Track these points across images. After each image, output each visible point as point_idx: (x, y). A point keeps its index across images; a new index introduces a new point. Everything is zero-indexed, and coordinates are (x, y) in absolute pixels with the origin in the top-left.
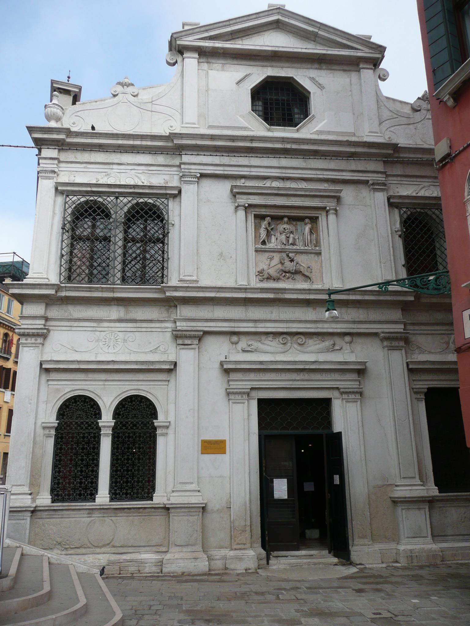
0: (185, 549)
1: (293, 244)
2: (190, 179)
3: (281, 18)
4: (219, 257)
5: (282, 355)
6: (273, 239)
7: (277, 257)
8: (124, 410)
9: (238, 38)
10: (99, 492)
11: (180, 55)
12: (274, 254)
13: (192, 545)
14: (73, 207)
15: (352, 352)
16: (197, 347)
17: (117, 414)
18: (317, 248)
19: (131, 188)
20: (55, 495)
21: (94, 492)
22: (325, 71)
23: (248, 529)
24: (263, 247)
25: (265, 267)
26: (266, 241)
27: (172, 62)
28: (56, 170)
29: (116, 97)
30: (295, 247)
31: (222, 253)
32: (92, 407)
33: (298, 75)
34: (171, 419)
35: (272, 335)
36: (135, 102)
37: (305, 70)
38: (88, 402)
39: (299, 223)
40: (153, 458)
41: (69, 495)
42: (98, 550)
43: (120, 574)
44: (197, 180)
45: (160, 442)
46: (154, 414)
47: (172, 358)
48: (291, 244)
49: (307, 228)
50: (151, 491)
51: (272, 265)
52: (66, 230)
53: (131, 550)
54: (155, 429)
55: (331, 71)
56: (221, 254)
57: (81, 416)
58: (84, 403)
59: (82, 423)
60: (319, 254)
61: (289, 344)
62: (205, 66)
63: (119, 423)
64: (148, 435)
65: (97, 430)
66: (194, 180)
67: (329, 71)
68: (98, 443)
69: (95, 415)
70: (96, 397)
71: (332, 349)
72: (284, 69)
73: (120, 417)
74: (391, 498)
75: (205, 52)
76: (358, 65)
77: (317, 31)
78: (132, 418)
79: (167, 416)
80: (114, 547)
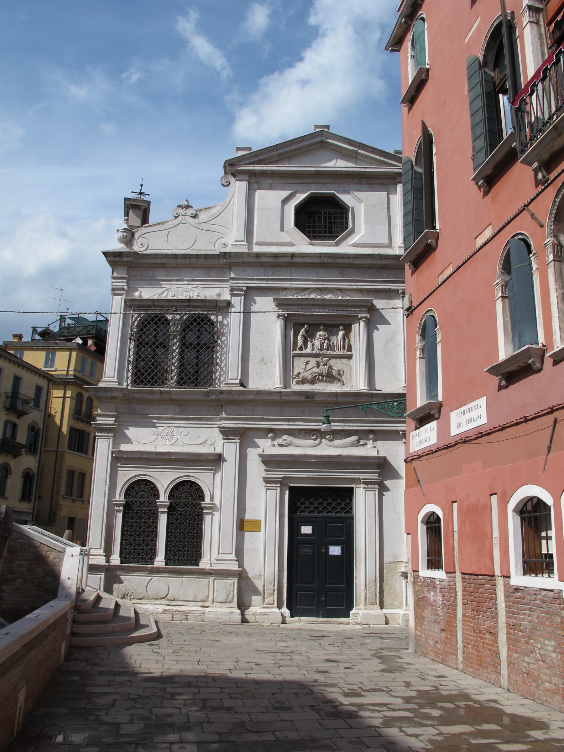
0: (223, 605)
1: (327, 349)
2: (238, 293)
3: (324, 139)
4: (261, 362)
5: (312, 449)
6: (309, 345)
7: (313, 362)
8: (178, 493)
9: (285, 158)
10: (157, 558)
11: (233, 178)
12: (310, 359)
13: (229, 603)
14: (138, 320)
15: (375, 447)
16: (239, 441)
17: (171, 496)
18: (349, 353)
19: (187, 302)
20: (124, 558)
21: (153, 557)
22: (365, 185)
23: (276, 592)
24: (300, 352)
25: (302, 372)
26: (303, 347)
27: (226, 184)
28: (126, 287)
29: (178, 219)
30: (328, 352)
31: (263, 358)
32: (152, 489)
33: (339, 190)
34: (217, 501)
35: (304, 432)
36: (193, 223)
37: (345, 185)
38: (148, 485)
39: (334, 329)
40: (200, 533)
41: (134, 558)
42: (157, 602)
43: (172, 620)
44: (243, 293)
45: (207, 519)
46: (201, 496)
47: (219, 450)
48: (325, 349)
49: (341, 333)
50: (198, 558)
51: (308, 368)
52: (132, 340)
53: (181, 603)
54: (202, 509)
55: (370, 185)
56: (263, 359)
57: (143, 496)
58: (146, 486)
59: (144, 502)
60: (350, 358)
61: (319, 439)
62: (255, 186)
63: (173, 503)
64: (196, 513)
65: (156, 508)
66: (241, 293)
67: (368, 186)
68: (157, 518)
69: (155, 495)
70: (156, 481)
71: (357, 444)
72: (327, 185)
73: (175, 498)
74: (399, 572)
75: (255, 173)
76: (395, 178)
77: (357, 150)
78: (184, 499)
79: (212, 498)
80: (168, 600)
